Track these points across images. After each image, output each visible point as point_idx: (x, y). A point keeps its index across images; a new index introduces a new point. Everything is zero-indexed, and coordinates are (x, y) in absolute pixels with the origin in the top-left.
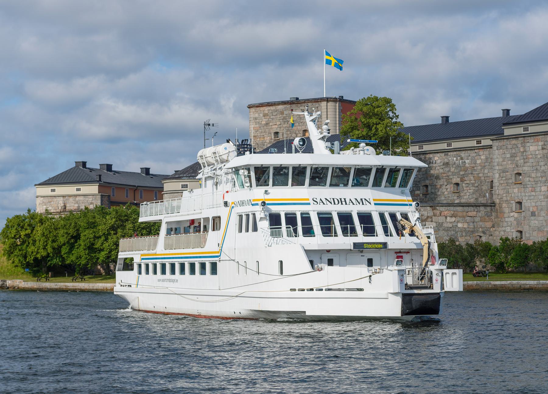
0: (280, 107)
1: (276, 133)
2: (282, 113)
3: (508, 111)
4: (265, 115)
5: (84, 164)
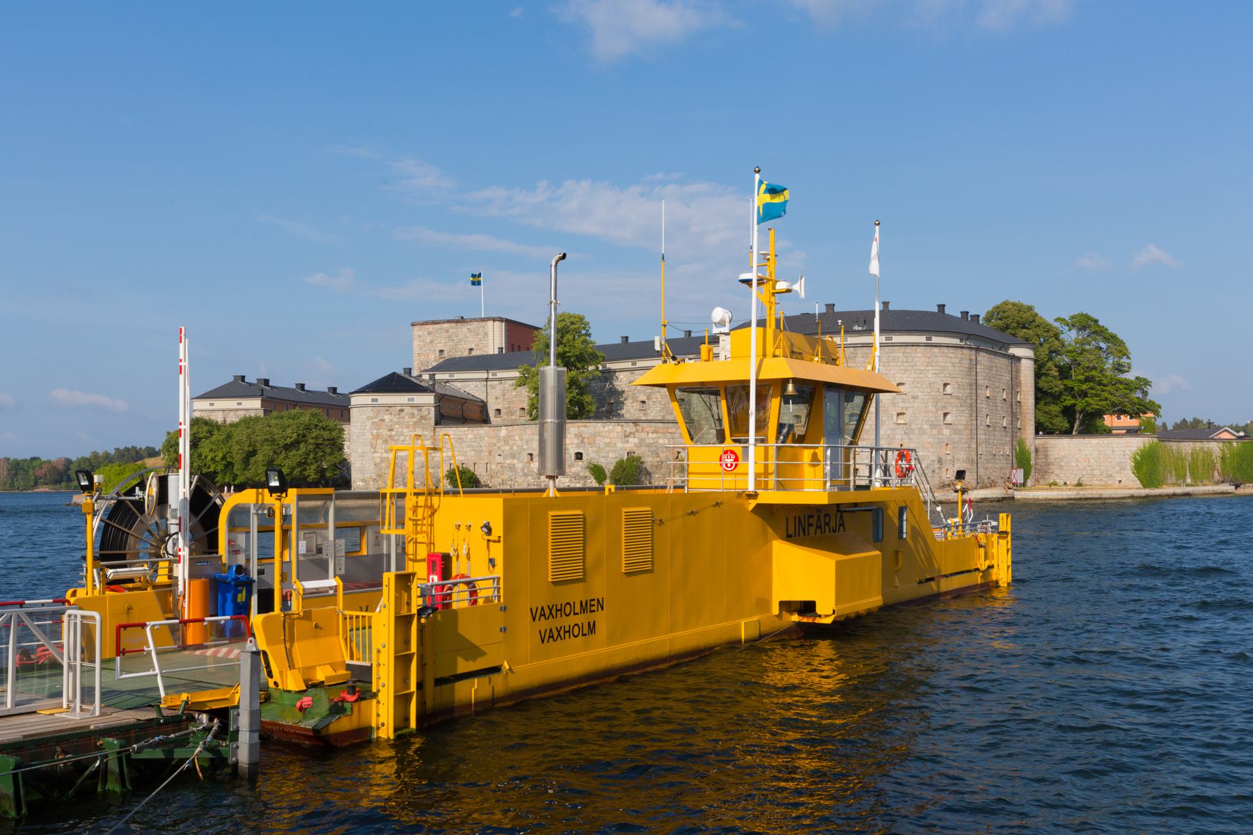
0: (446, 325)
1: (441, 351)
2: (447, 331)
3: (690, 332)
4: (429, 333)
5: (243, 378)
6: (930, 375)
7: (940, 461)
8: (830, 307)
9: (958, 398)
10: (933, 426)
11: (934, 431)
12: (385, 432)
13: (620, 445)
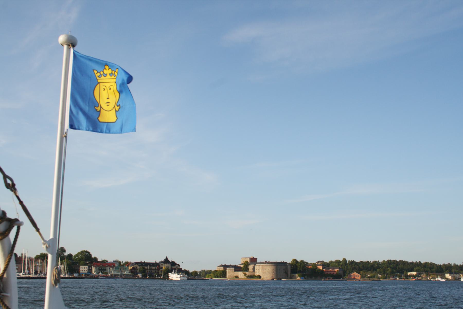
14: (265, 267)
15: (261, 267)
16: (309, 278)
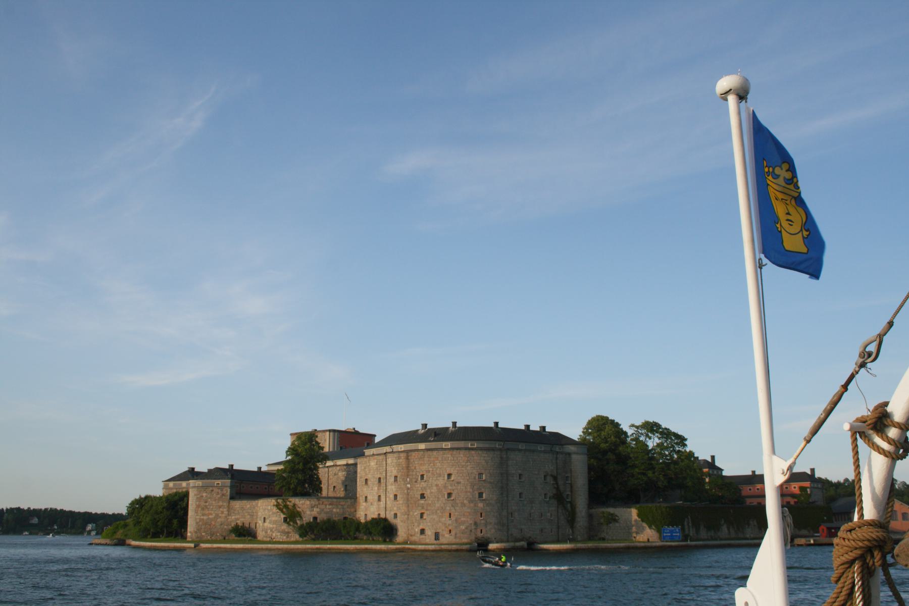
6: (468, 468)
7: (476, 524)
8: (425, 426)
9: (490, 483)
10: (471, 501)
11: (472, 505)
12: (203, 504)
13: (308, 512)
14: (420, 466)
15: (393, 466)
16: (703, 533)
